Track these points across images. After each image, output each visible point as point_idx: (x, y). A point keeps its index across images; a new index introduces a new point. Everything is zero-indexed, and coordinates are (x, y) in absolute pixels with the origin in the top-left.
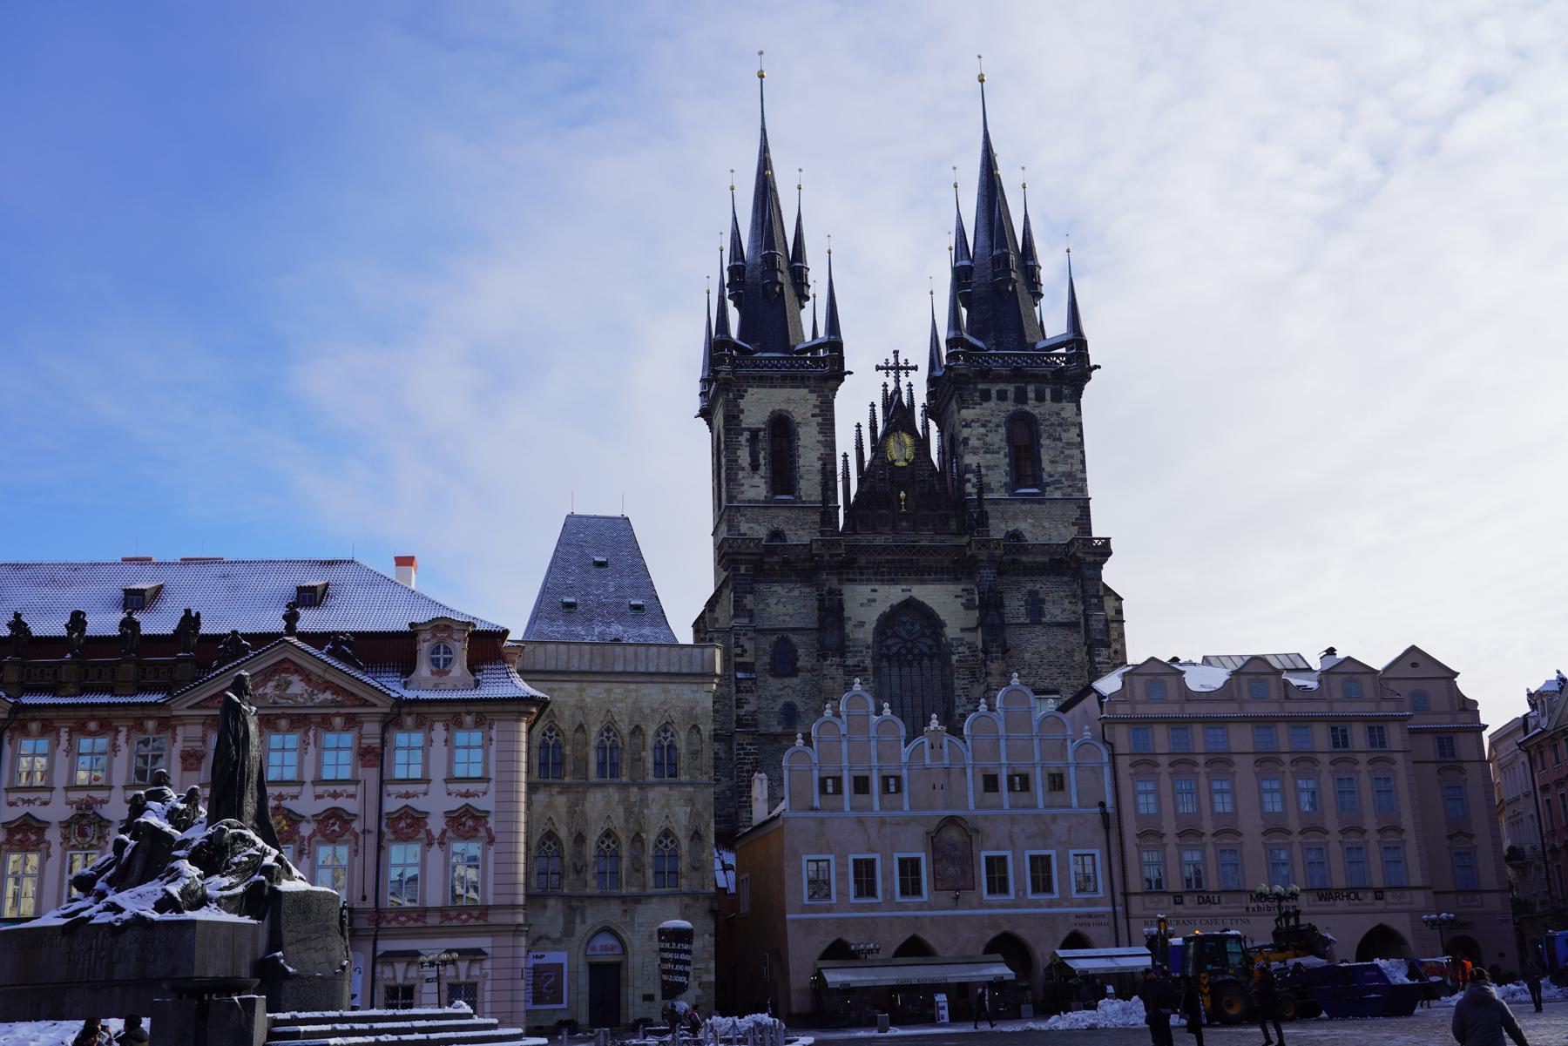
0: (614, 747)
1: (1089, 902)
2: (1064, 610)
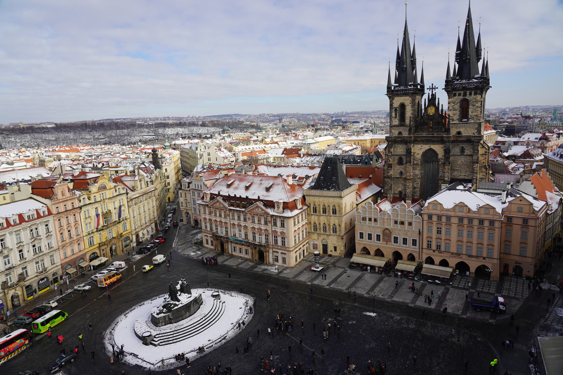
1: (414, 248)
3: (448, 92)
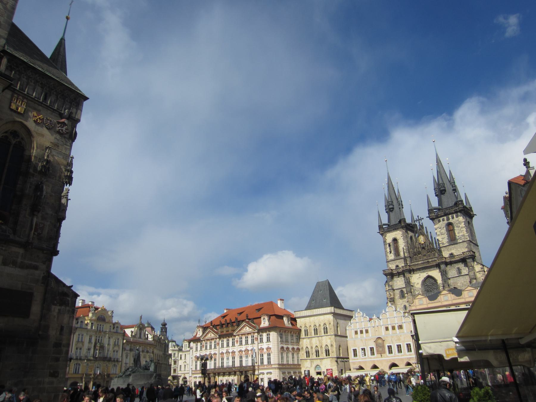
0: (317, 329)
1: (410, 355)
2: (467, 271)
3: (432, 219)
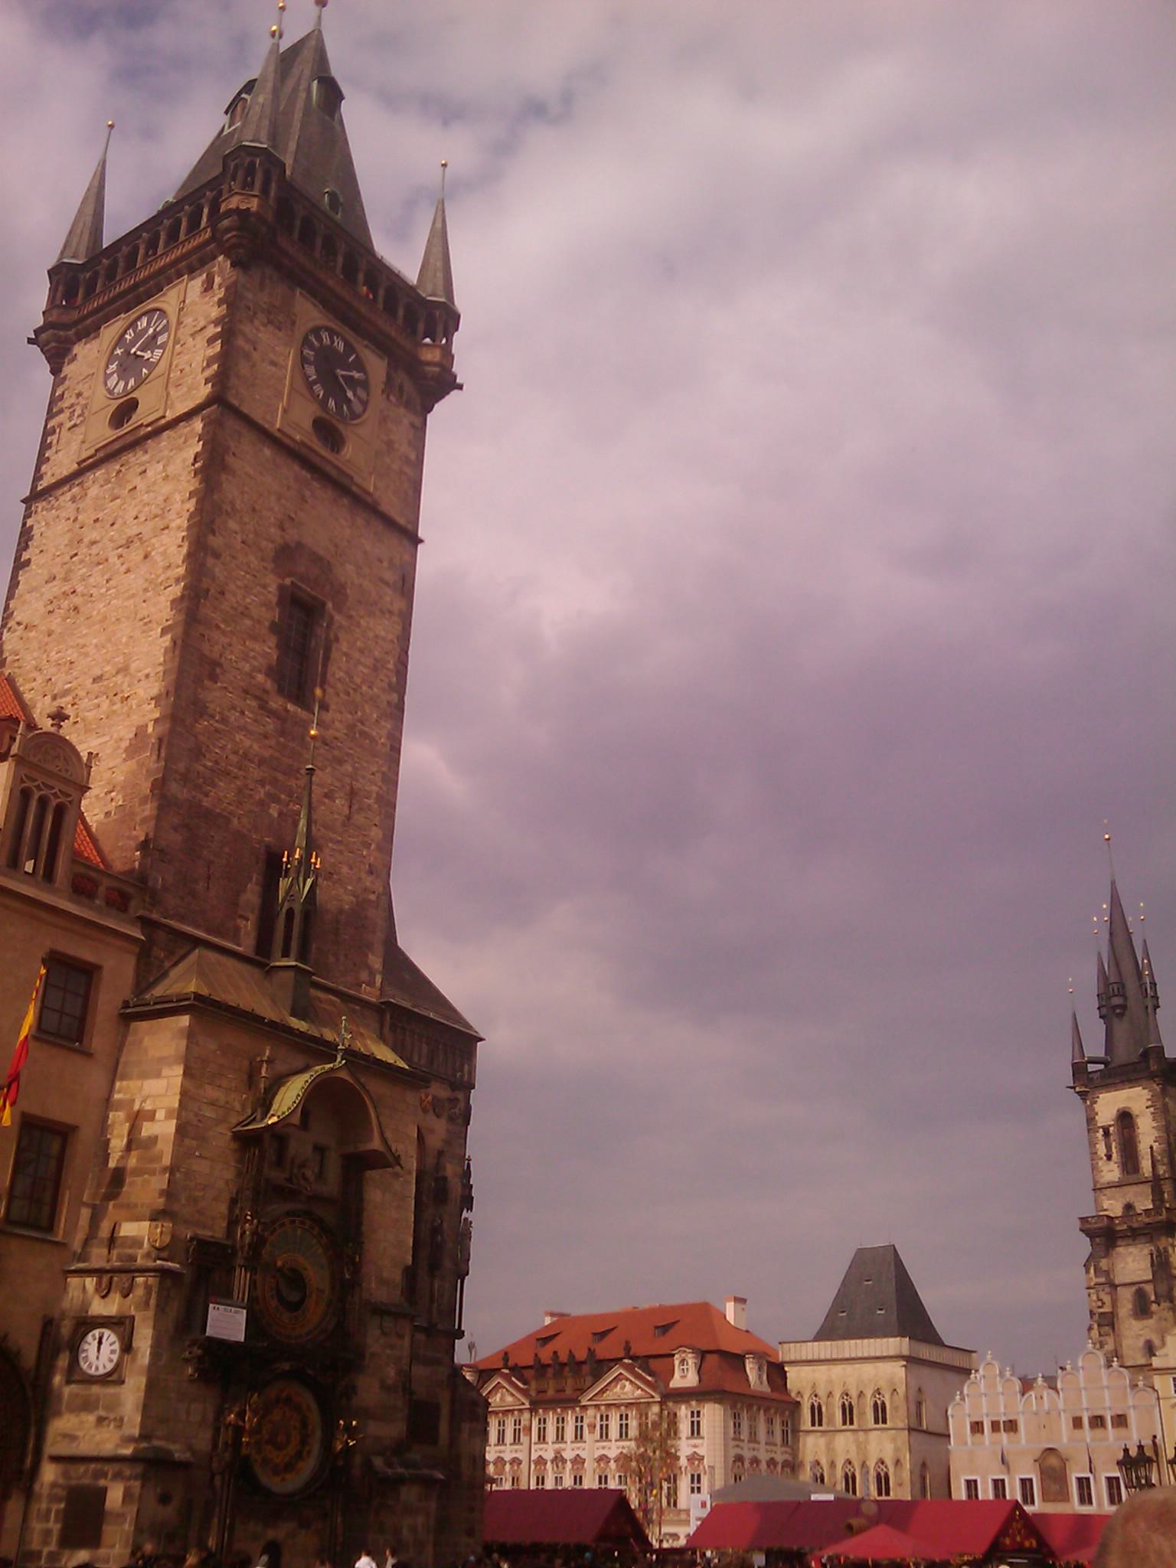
0: (850, 1403)
